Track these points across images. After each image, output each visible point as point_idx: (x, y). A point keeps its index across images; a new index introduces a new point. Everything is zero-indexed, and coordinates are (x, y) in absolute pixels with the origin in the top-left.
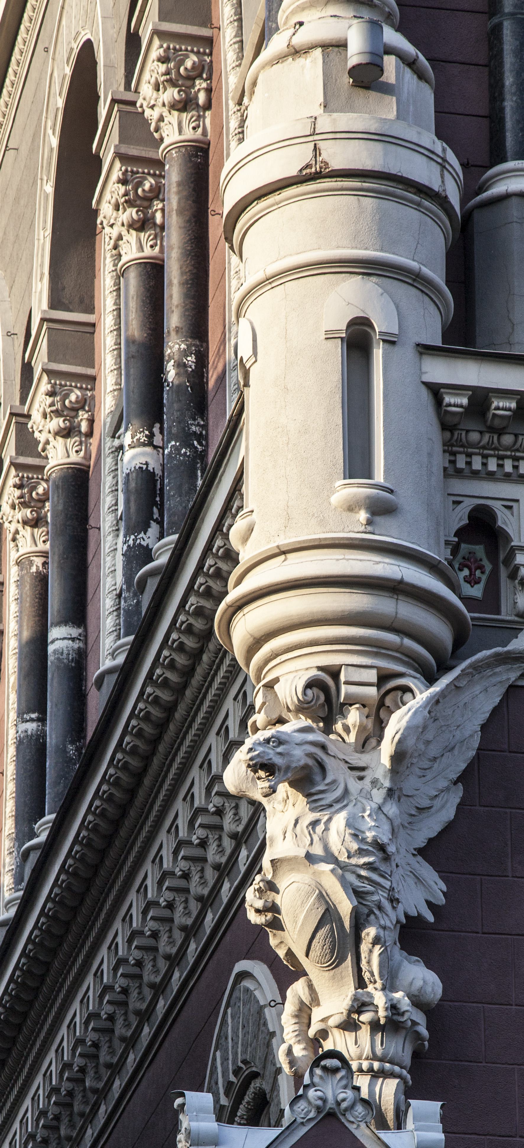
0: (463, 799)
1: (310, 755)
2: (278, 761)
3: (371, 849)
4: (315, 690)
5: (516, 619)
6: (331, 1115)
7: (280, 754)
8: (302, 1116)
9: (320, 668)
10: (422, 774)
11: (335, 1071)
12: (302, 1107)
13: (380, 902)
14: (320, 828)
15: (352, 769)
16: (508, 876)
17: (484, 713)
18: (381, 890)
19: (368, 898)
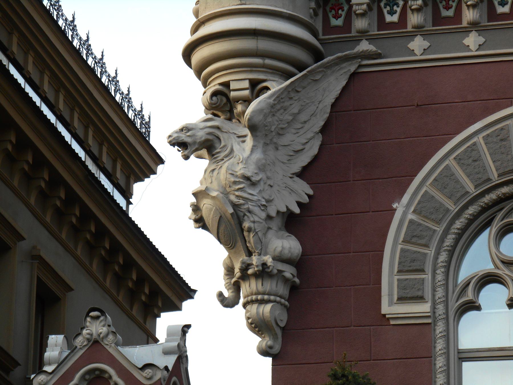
0: (322, 142)
1: (209, 134)
2: (188, 140)
3: (241, 180)
4: (219, 97)
5: (357, 34)
6: (96, 342)
7: (189, 136)
8: (80, 344)
9: (220, 84)
10: (295, 132)
11: (97, 318)
12: (80, 340)
13: (249, 208)
14: (216, 172)
15: (239, 137)
16: (350, 181)
17: (337, 91)
18: (250, 202)
19: (241, 208)
